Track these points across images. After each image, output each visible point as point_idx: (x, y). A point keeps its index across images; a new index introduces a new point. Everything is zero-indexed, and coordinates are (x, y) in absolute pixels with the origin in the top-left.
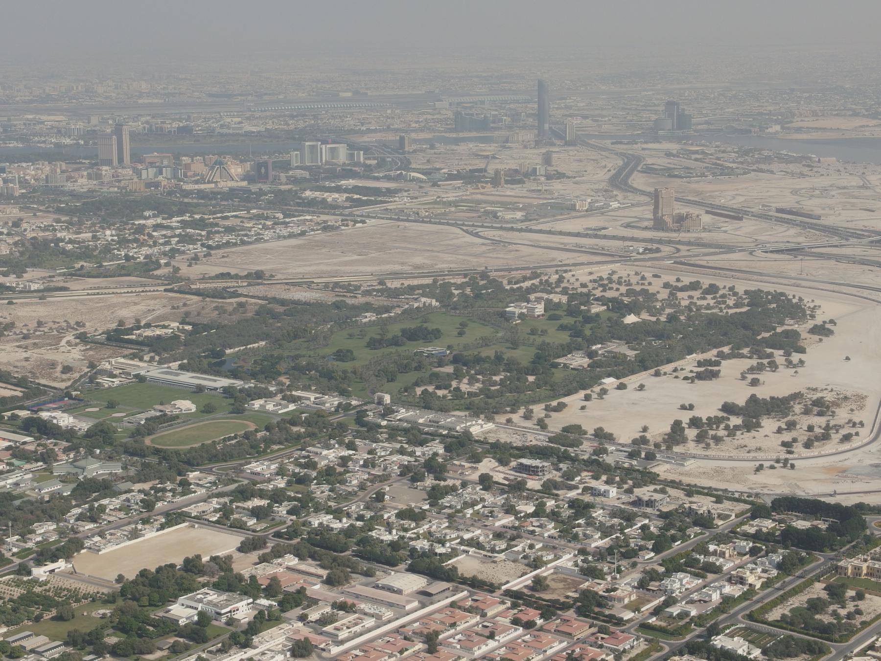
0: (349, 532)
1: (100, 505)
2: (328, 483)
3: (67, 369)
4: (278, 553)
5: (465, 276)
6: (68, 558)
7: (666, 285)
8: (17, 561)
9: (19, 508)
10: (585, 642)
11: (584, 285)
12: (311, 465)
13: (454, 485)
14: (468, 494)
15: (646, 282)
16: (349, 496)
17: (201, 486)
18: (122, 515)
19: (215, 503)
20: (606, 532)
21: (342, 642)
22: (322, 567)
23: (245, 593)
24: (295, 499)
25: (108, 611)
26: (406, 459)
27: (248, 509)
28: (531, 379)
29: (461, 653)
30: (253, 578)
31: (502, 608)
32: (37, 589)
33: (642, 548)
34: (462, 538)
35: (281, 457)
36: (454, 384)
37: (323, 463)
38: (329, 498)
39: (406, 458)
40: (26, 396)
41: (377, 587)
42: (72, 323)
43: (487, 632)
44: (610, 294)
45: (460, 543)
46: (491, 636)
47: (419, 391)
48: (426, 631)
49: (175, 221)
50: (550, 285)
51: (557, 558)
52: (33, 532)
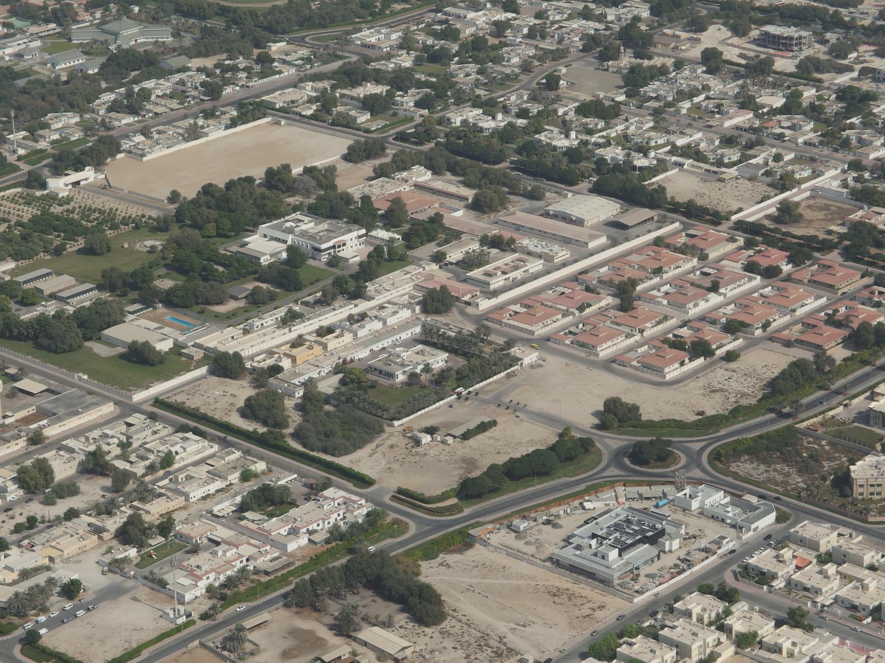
0: (506, 134)
1: (142, 90)
2: (476, 61)
4: (402, 164)
6: (98, 165)
8: (25, 168)
9: (24, 91)
10: (853, 299)
12: (451, 34)
13: (663, 66)
14: (684, 79)
16: (507, 81)
17: (289, 63)
18: (174, 104)
19: (309, 89)
21: (495, 293)
22: (467, 184)
23: (355, 220)
24: (427, 84)
25: (158, 243)
26: (591, 26)
27: (357, 99)
29: (669, 311)
30: (366, 199)
31: (730, 247)
32: (56, 209)
34: (674, 145)
35: (407, 21)
37: (469, 31)
38: (477, 84)
39: (591, 24)
41: (547, 215)
43: (707, 282)
46: (714, 288)
48: (617, 279)
51: (816, 174)
52: (46, 126)
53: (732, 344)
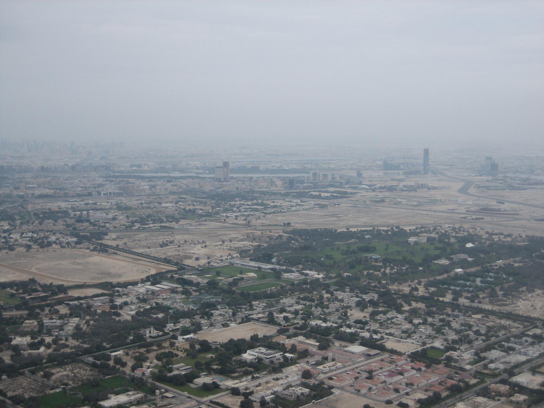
1: (211, 313)
3: (197, 259)
4: (295, 335)
5: (388, 227)
6: (195, 332)
7: (487, 233)
8: (171, 333)
11: (446, 231)
15: (477, 231)
17: (259, 307)
20: (457, 332)
22: (317, 342)
25: (214, 356)
28: (421, 268)
30: (283, 345)
33: (477, 339)
36: (382, 270)
38: (321, 314)
40: (179, 270)
42: (201, 241)
44: (458, 235)
45: (386, 334)
47: (365, 273)
49: (249, 203)
50: (429, 230)
52: (179, 322)
53: (408, 390)
